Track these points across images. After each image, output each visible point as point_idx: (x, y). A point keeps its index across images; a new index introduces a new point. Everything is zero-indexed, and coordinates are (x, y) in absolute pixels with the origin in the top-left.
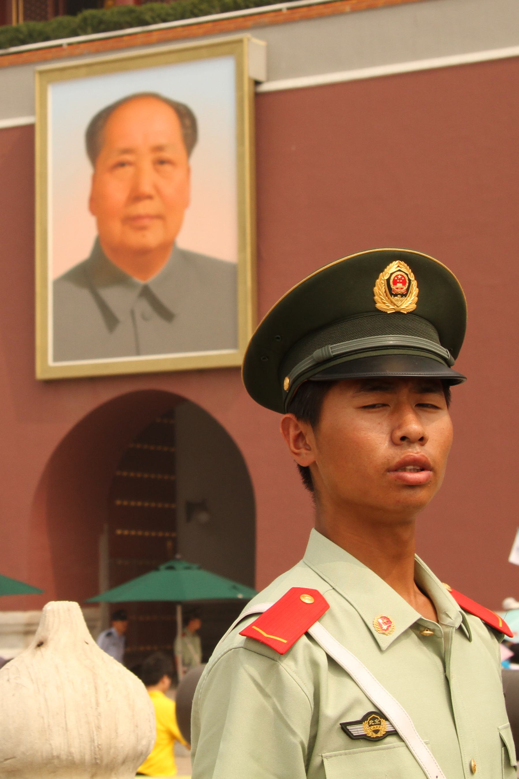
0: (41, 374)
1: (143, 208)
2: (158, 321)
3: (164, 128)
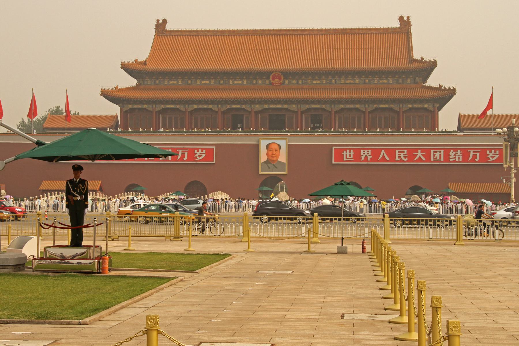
3: (277, 147)
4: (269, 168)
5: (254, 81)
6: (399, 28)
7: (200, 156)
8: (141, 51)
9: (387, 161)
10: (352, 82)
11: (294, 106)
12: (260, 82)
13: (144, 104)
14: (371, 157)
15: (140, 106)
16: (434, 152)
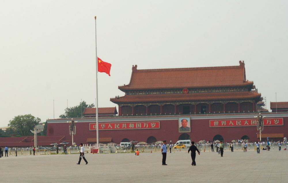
4: (183, 130)
5: (176, 92)
6: (240, 66)
7: (153, 126)
8: (127, 81)
9: (232, 125)
10: (218, 91)
11: (193, 103)
12: (178, 92)
13: (128, 104)
14: (226, 124)
15: (127, 105)
16: (252, 121)
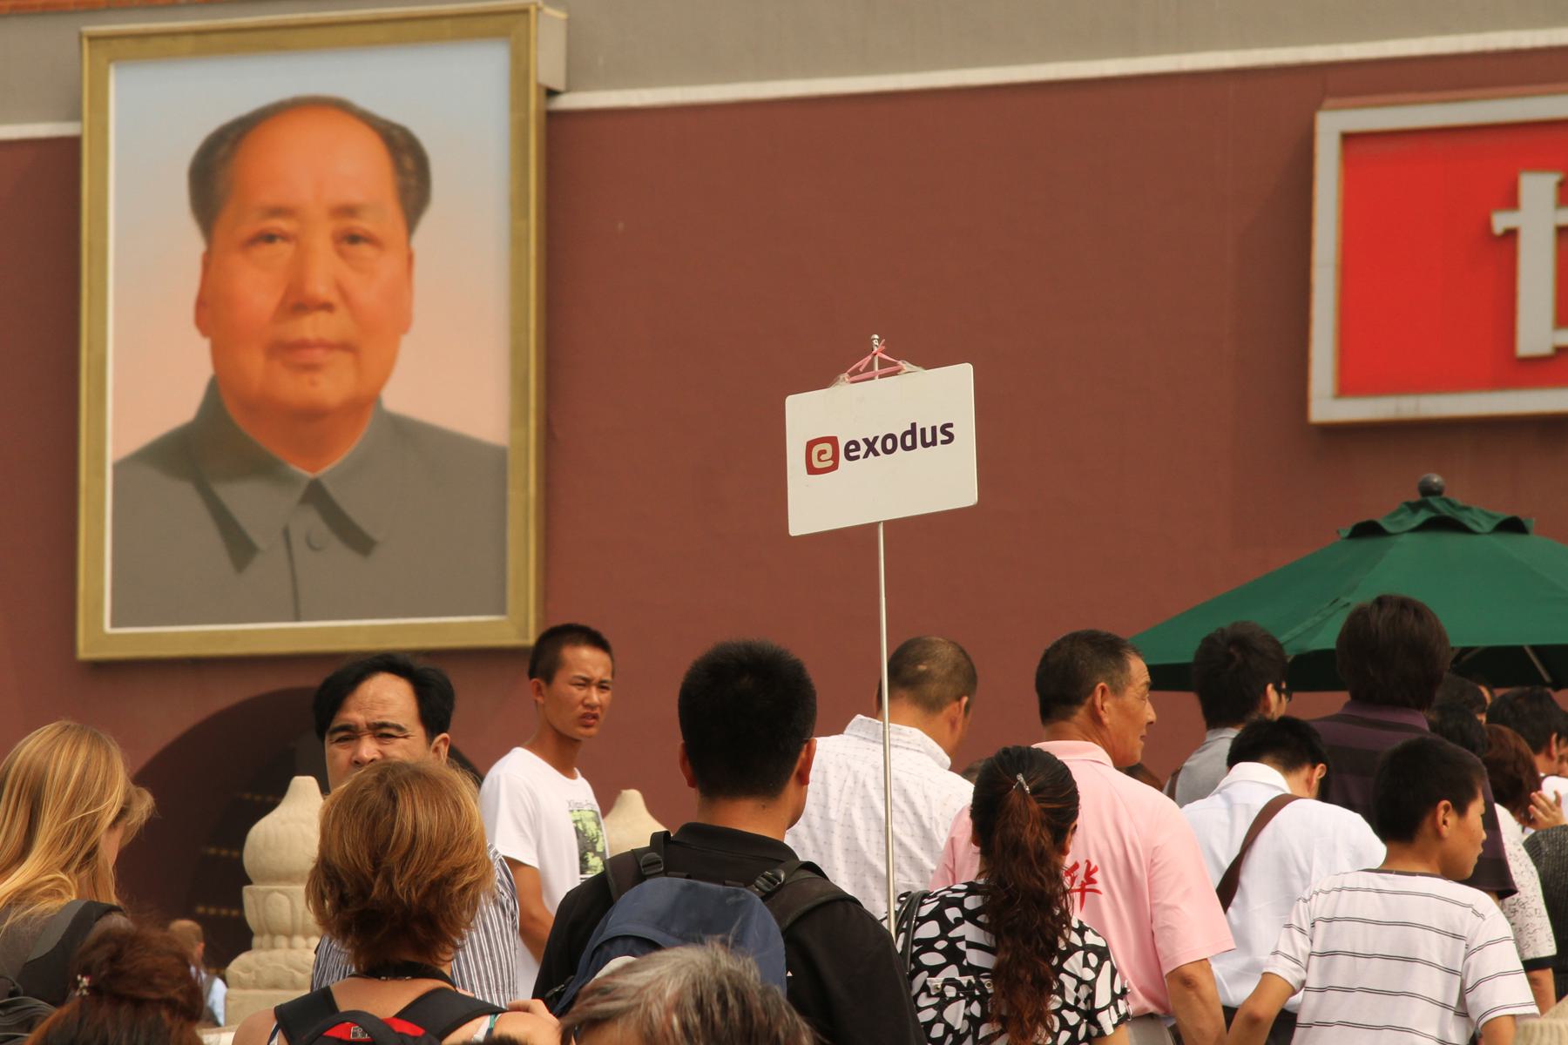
0: (86, 649)
1: (312, 327)
2: (339, 554)
3: (360, 171)
4: (240, 547)
